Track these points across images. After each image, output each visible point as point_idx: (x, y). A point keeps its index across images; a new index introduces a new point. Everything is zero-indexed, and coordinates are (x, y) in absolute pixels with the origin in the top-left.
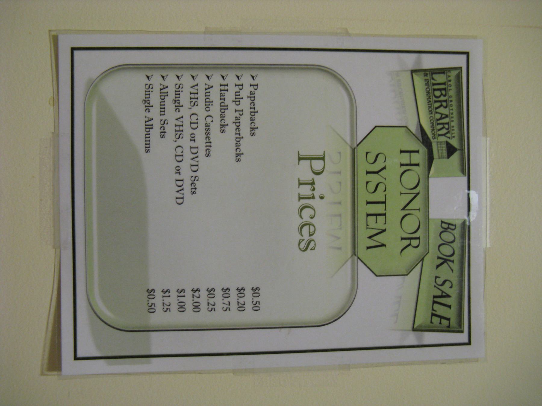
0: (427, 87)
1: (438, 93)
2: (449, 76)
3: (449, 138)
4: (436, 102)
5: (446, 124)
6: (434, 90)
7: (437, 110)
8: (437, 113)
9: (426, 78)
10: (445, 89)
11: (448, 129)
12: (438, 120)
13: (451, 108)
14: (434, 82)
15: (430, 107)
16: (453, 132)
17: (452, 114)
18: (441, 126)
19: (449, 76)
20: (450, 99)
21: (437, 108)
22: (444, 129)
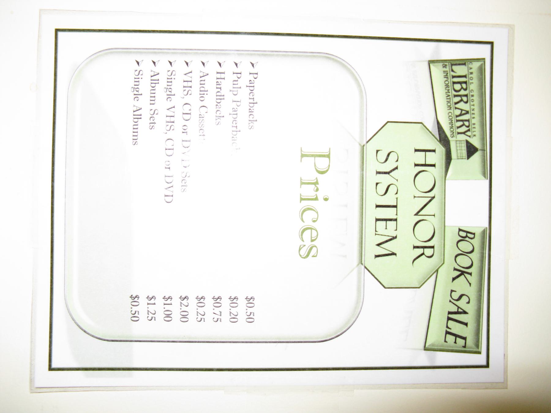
0: (446, 79)
1: (457, 87)
2: (471, 68)
3: (470, 136)
4: (455, 96)
5: (466, 121)
6: (454, 83)
7: (457, 106)
8: (456, 108)
9: (445, 69)
10: (465, 83)
11: (468, 127)
12: (457, 116)
13: (472, 103)
14: (454, 74)
15: (448, 102)
16: (474, 130)
17: (473, 110)
18: (461, 123)
19: (471, 68)
20: (471, 94)
21: (456, 103)
22: (464, 127)
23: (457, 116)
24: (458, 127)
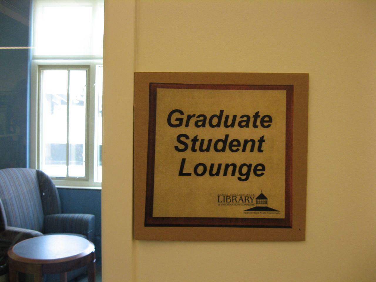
0: (225, 205)
1: (229, 200)
2: (221, 194)
3: (254, 197)
4: (233, 202)
6: (227, 202)
7: (238, 201)
8: (239, 202)
11: (249, 198)
12: (243, 202)
14: (223, 201)
16: (250, 195)
21: (236, 202)
22: (248, 199)
23: (243, 202)
24: (249, 202)
